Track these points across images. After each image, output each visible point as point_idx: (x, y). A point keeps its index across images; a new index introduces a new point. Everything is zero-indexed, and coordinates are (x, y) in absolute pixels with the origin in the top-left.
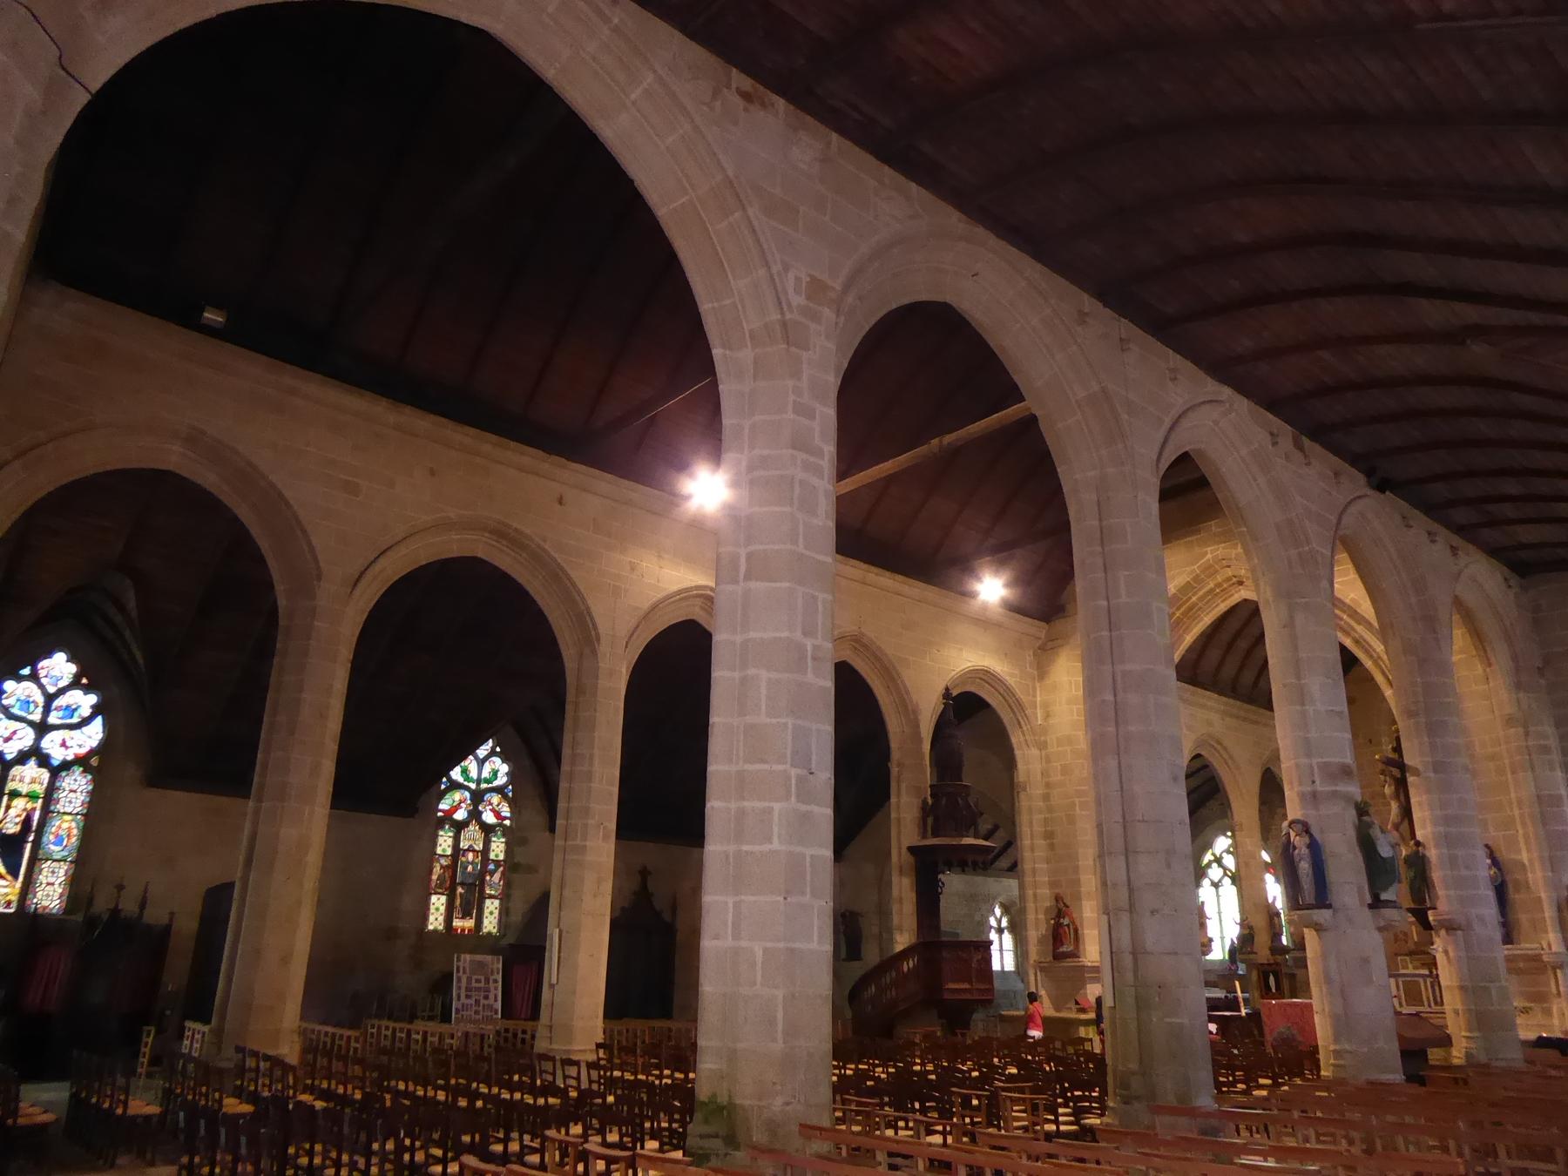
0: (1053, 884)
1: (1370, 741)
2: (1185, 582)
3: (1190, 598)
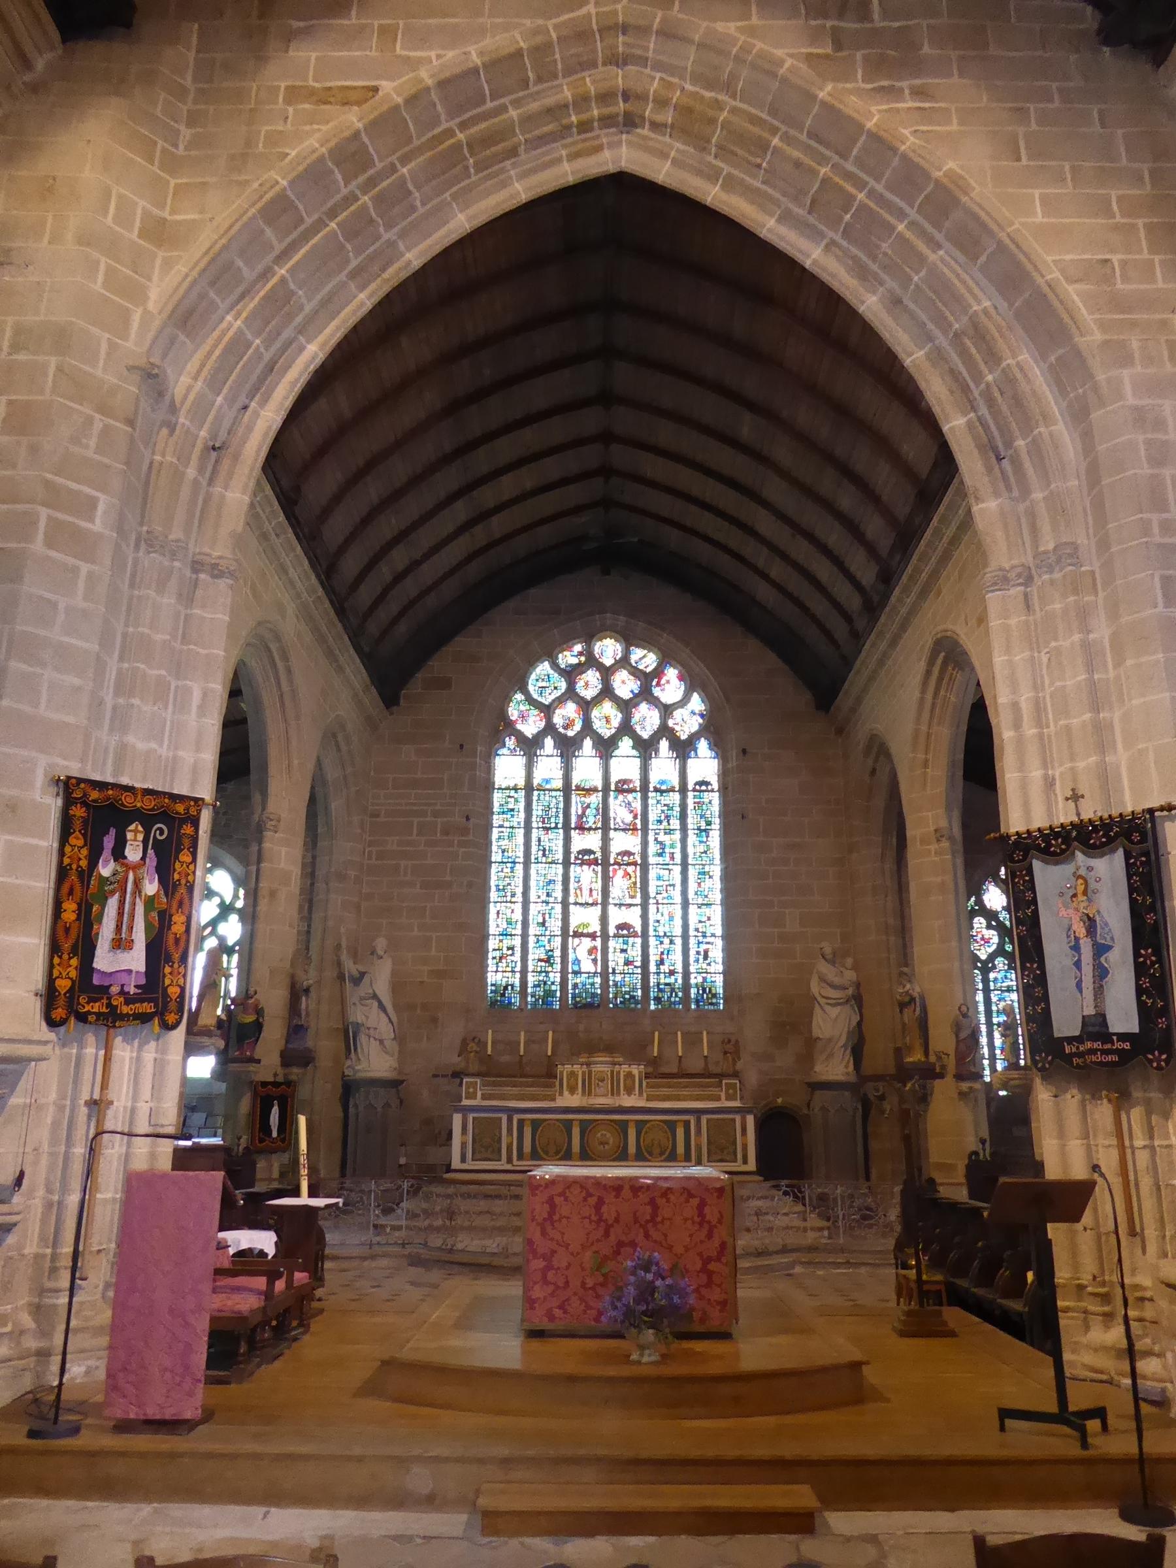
1: (462, 746)
2: (512, 49)
3: (503, 109)
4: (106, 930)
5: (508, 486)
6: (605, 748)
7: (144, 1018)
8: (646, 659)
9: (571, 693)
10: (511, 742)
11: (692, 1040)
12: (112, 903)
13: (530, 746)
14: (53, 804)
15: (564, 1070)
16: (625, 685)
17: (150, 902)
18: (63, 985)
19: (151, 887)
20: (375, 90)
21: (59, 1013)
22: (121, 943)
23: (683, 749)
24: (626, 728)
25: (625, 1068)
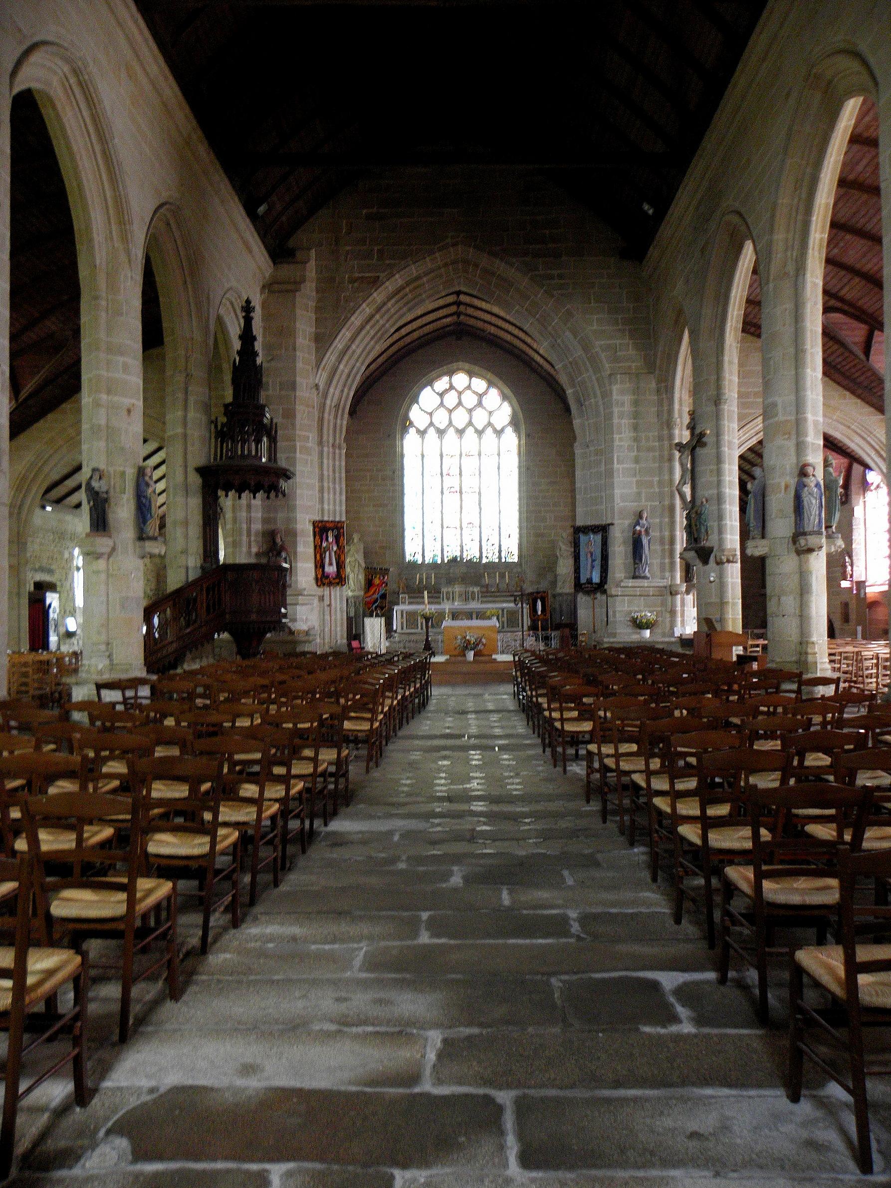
0: (265, 521)
6: (461, 432)
7: (338, 584)
8: (479, 384)
9: (442, 404)
10: (412, 431)
11: (502, 576)
12: (328, 553)
13: (422, 433)
14: (311, 528)
15: (444, 590)
16: (470, 400)
17: (335, 552)
18: (319, 576)
19: (335, 548)
20: (378, 277)
22: (331, 564)
23: (499, 433)
24: (470, 423)
25: (471, 589)
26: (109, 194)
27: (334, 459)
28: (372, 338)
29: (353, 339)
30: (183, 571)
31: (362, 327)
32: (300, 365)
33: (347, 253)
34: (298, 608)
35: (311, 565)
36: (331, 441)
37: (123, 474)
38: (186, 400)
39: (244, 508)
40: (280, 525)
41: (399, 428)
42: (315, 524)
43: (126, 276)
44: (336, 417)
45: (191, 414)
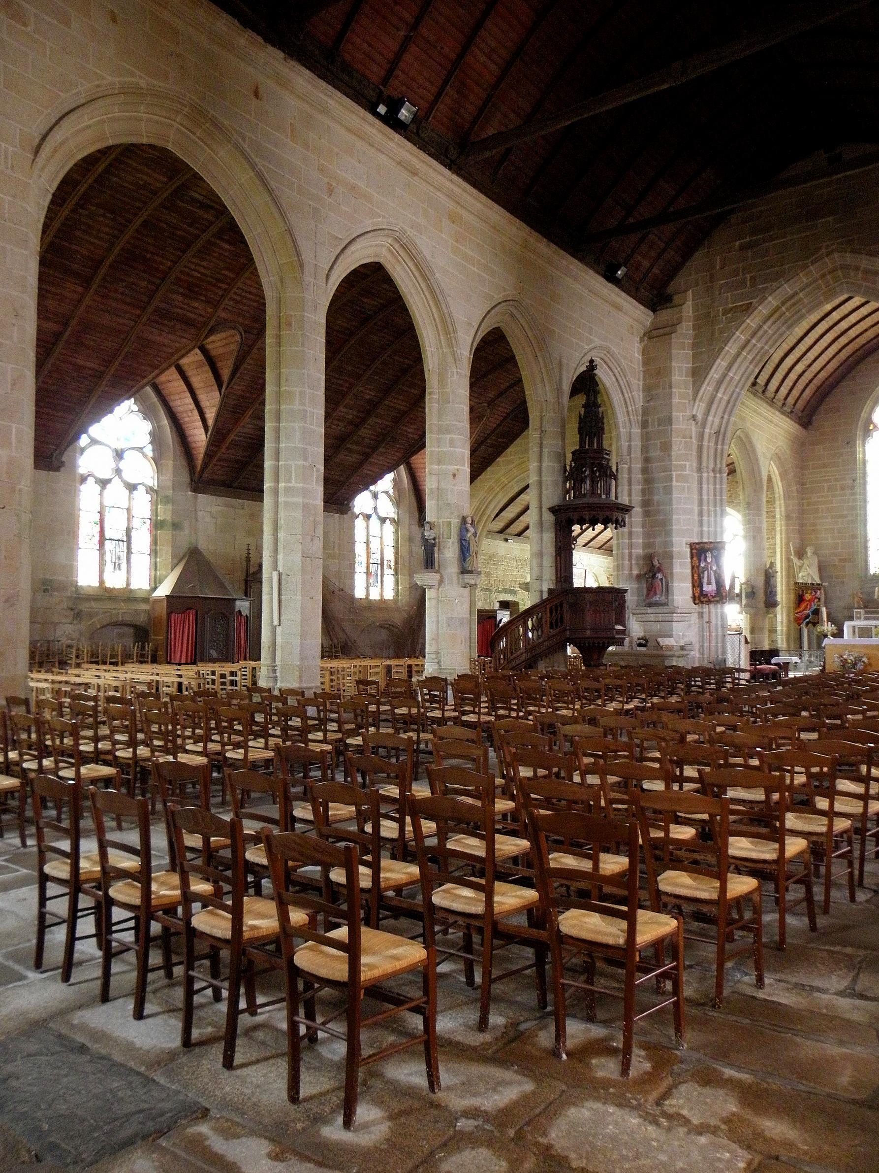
0: (646, 546)
4: (705, 580)
5: (853, 318)
14: (688, 550)
21: (697, 602)
22: (709, 583)
26: (436, 315)
27: (715, 484)
28: (751, 363)
29: (729, 368)
30: (538, 594)
31: (738, 355)
32: (675, 400)
33: (722, 286)
34: (674, 624)
35: (689, 585)
36: (711, 466)
37: (450, 523)
38: (541, 452)
39: (626, 536)
40: (659, 549)
41: (859, 433)
42: (692, 546)
43: (452, 372)
44: (716, 443)
45: (546, 464)
